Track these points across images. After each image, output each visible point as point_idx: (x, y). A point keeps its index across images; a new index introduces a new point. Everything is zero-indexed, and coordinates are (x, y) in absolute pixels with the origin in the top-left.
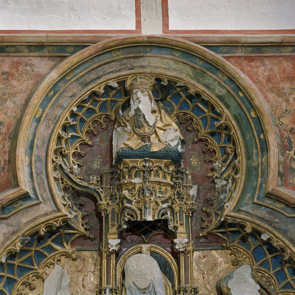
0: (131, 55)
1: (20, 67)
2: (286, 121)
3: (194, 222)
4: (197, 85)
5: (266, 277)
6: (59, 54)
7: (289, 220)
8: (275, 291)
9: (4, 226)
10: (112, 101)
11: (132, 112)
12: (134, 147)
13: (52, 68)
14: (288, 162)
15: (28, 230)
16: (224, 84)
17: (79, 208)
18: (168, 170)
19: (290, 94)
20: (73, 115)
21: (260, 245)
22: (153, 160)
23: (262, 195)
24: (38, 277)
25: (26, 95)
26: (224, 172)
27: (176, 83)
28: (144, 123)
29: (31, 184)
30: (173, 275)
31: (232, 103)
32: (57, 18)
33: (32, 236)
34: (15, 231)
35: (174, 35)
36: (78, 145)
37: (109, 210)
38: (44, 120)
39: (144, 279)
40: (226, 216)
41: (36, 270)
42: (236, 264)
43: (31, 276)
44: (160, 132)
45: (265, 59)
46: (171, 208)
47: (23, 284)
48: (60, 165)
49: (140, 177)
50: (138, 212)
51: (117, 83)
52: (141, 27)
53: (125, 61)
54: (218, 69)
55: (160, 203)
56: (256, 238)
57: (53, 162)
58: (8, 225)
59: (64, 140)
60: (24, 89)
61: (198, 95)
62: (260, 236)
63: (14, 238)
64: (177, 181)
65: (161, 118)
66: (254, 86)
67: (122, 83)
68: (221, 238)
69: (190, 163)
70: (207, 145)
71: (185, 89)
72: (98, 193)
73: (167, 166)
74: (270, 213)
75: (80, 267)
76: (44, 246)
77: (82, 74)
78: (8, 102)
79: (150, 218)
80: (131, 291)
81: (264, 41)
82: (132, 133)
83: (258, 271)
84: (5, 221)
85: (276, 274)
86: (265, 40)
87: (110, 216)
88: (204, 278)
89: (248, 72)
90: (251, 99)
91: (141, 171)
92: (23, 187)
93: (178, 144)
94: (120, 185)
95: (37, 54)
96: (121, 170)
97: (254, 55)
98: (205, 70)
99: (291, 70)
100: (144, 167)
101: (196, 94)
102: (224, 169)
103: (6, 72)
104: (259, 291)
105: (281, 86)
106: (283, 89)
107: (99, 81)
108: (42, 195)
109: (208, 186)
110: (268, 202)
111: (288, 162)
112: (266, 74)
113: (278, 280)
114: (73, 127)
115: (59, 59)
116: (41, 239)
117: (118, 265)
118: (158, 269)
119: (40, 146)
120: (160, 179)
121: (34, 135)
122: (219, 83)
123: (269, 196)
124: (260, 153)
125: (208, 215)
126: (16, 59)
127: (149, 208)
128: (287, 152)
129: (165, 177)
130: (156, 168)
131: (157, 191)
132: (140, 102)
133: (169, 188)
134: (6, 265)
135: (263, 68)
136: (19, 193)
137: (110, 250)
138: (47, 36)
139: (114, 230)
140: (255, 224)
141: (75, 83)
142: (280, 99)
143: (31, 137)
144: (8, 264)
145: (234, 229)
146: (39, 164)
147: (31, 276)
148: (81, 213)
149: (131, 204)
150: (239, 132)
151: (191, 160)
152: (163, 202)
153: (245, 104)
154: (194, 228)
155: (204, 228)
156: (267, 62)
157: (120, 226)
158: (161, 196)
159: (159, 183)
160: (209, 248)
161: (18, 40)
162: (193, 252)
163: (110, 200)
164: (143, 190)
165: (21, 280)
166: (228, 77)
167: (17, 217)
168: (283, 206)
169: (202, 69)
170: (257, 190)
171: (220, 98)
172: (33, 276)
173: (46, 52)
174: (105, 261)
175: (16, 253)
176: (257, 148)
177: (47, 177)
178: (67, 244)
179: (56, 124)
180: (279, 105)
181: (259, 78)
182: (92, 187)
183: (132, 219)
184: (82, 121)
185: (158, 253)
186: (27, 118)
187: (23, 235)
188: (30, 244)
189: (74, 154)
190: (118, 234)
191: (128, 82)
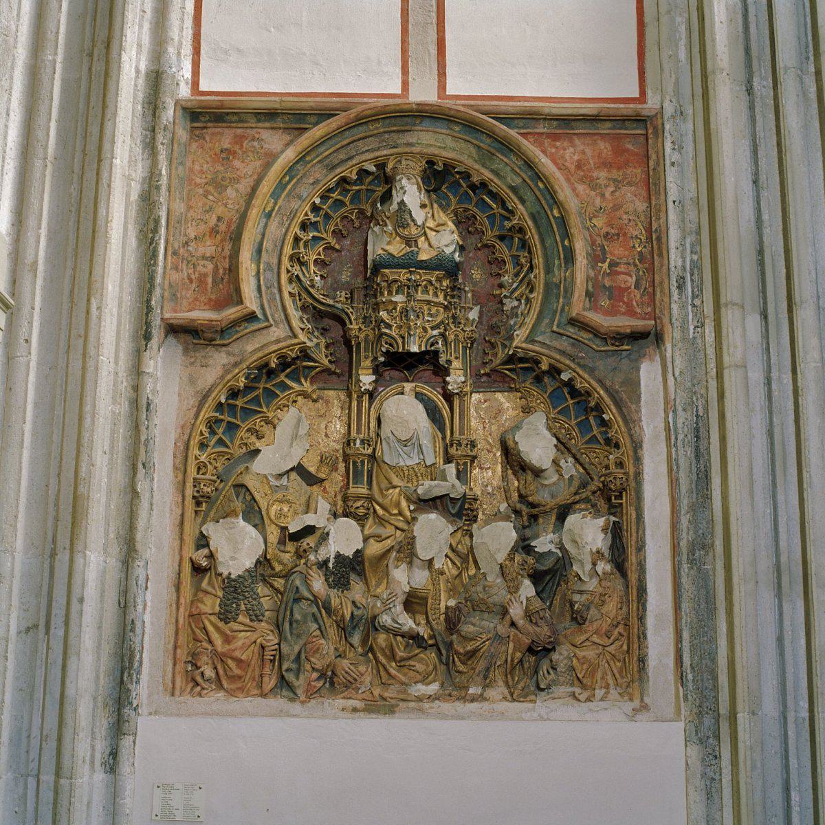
0: (395, 128)
1: (245, 142)
2: (599, 222)
3: (473, 355)
4: (483, 170)
5: (565, 429)
6: (297, 126)
7: (597, 354)
8: (577, 446)
9: (223, 355)
10: (367, 190)
11: (394, 206)
12: (395, 253)
13: (287, 145)
14: (600, 278)
15: (255, 361)
16: (518, 171)
17: (322, 334)
18: (441, 285)
19: (606, 186)
20: (315, 209)
21: (559, 387)
22: (421, 271)
23: (564, 320)
24: (268, 422)
25: (252, 180)
26: (515, 289)
27: (454, 168)
28: (410, 222)
29: (258, 301)
30: (445, 424)
31: (528, 196)
32: (295, 76)
33: (260, 368)
35: (453, 102)
36: (321, 249)
37: (362, 336)
38: (276, 215)
39: (405, 427)
40: (516, 348)
42: (527, 410)
43: (258, 420)
44: (431, 234)
45: (575, 138)
46: (443, 335)
47: (248, 430)
48: (297, 276)
49: (403, 294)
50: (400, 341)
51: (375, 166)
52: (408, 89)
53: (386, 136)
54: (511, 150)
55: (429, 329)
56: (554, 378)
57: (288, 271)
58: (228, 354)
59: (302, 242)
60: (250, 173)
61: (484, 185)
62: (559, 375)
63: (237, 371)
64: (452, 300)
65: (433, 215)
66: (558, 174)
67: (381, 166)
68: (509, 376)
69: (471, 277)
70: (494, 253)
71: (466, 175)
72: (347, 314)
73: (439, 280)
74: (573, 345)
75: (322, 412)
77: (327, 153)
78: (229, 190)
79: (414, 349)
80: (388, 443)
81: (574, 113)
82: (394, 235)
83: (555, 420)
84: (224, 349)
85: (578, 424)
86: (575, 112)
87: (362, 345)
88: (484, 427)
89: (552, 154)
90: (554, 192)
91: (405, 285)
92: (248, 305)
93: (455, 251)
94: (377, 304)
95: (267, 125)
96: (378, 285)
97: (561, 131)
98: (493, 151)
99: (609, 153)
100: (409, 280)
101: (481, 184)
102: (515, 285)
103: (226, 150)
104: (556, 446)
105: (595, 174)
106: (598, 179)
107: (350, 163)
108: (272, 316)
109: (494, 308)
110: (571, 331)
111: (600, 278)
112: (576, 158)
113: (581, 432)
114: (315, 225)
115: (296, 133)
116: (271, 373)
117: (372, 409)
118: (425, 415)
119: (270, 249)
120: (430, 297)
121: (263, 235)
122: (513, 169)
123: (573, 322)
124: (563, 265)
125: (493, 346)
126: (239, 131)
127: (414, 334)
128: (600, 264)
129: (436, 295)
130: (424, 283)
131: (426, 313)
132: (404, 193)
133: (442, 309)
134: (225, 406)
135: (572, 150)
137: (362, 390)
138: (282, 101)
139: (368, 363)
140: (554, 359)
141: (319, 165)
142: (593, 193)
143: (259, 237)
144: (228, 405)
145: (526, 365)
146: (269, 274)
147: (258, 420)
148: (324, 341)
149: (391, 330)
150: (536, 237)
151: (473, 272)
152: (433, 328)
153: (545, 199)
154: (474, 363)
155: (487, 363)
156: (577, 141)
157: (376, 359)
158: (430, 319)
159: (429, 302)
160: (493, 390)
161: (242, 105)
162: (471, 394)
163: (363, 323)
164: (407, 311)
165: (245, 426)
166: (525, 161)
168: (591, 336)
169: (490, 149)
170: (558, 315)
171: (514, 189)
172: (261, 421)
173: (279, 122)
174: (354, 404)
175: (239, 390)
176: (560, 258)
177: (280, 291)
178: (306, 380)
179: (292, 220)
180: (591, 201)
181: (566, 164)
182: (339, 306)
183: (392, 350)
184: (327, 217)
185: (425, 395)
186: (254, 213)
187: (248, 368)
188: (257, 379)
189: (315, 261)
190: (373, 369)
191: (390, 165)
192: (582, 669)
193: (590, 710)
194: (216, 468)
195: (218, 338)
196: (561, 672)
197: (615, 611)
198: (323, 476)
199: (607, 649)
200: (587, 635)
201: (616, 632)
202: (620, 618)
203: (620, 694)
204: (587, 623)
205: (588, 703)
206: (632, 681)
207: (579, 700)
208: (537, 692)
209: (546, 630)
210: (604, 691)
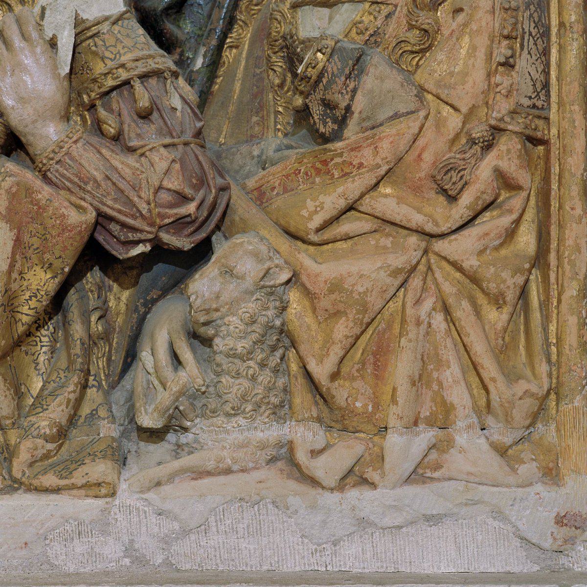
192: (328, 341)
193: (363, 523)
196: (232, 354)
197: (478, 76)
199: (439, 246)
200: (353, 187)
201: (484, 171)
202: (503, 107)
203: (502, 451)
204: (351, 131)
205: (353, 494)
206: (556, 391)
207: (314, 482)
208: (131, 445)
209: (162, 166)
210: (426, 436)
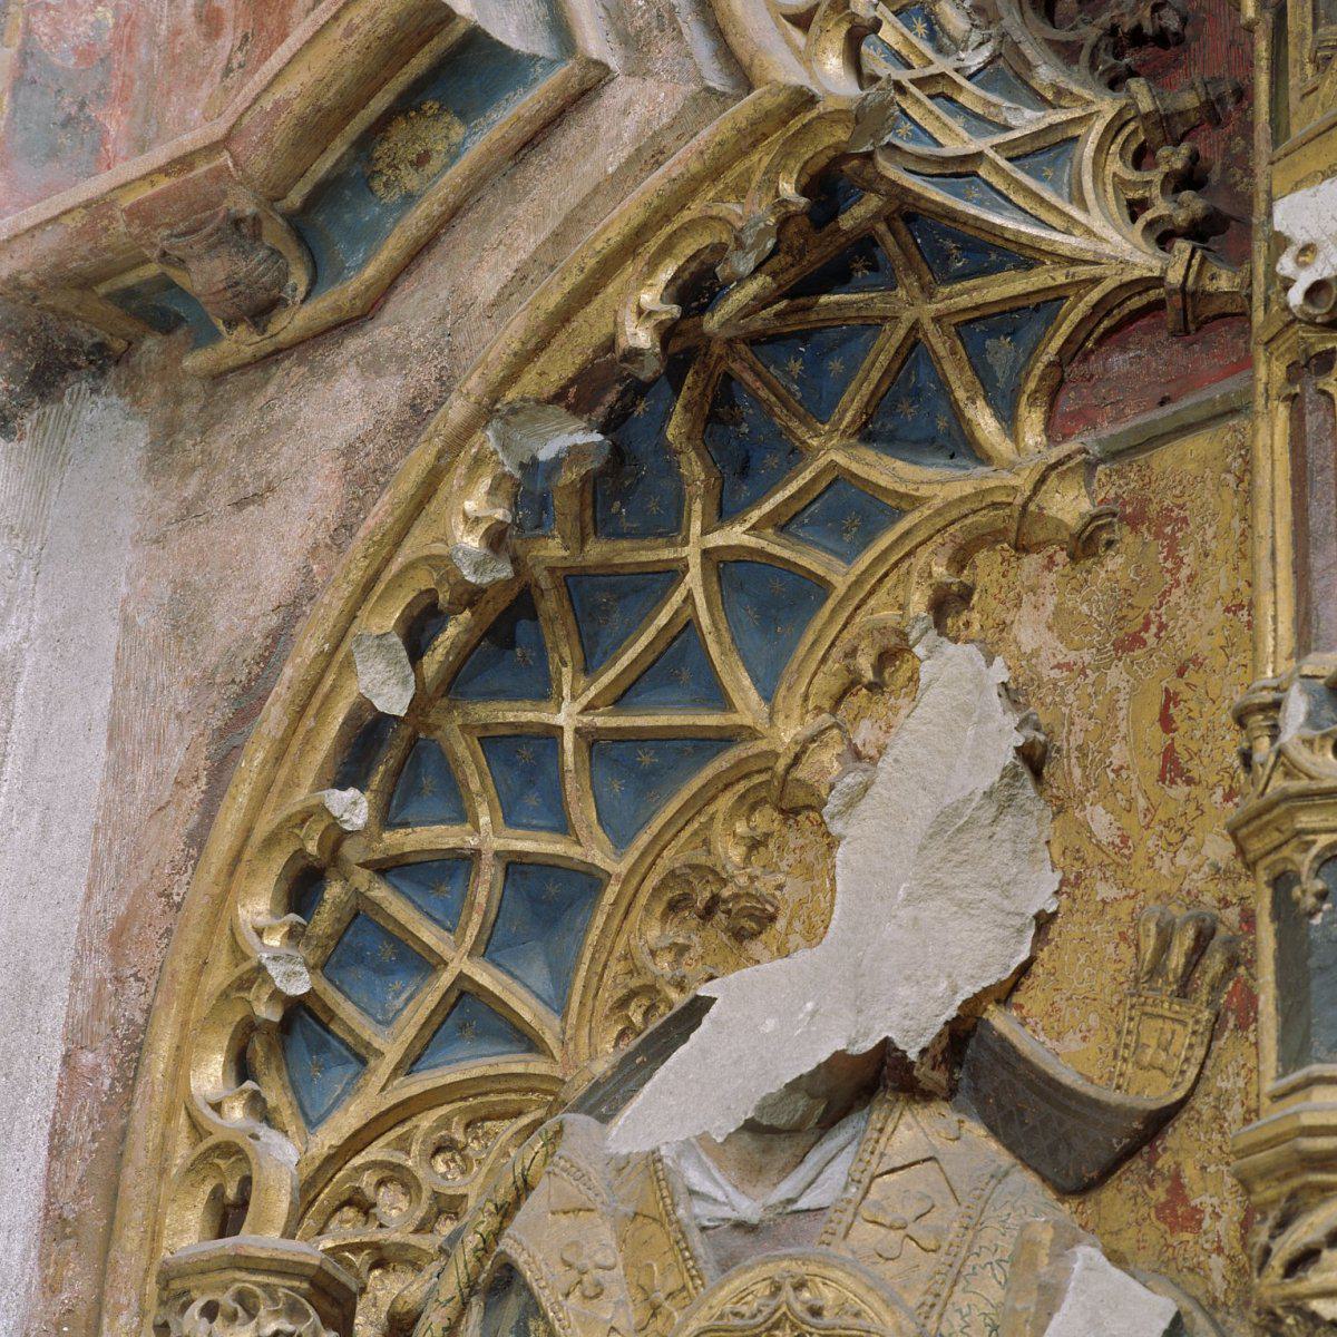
34: (422, 394)
41: (751, 734)
43: (725, 802)
76: (780, 497)
84: (355, 344)
136: (349, 33)
148: (1107, 107)
167: (442, 271)
178: (1009, 420)
194: (449, 1206)
195: (299, 278)
198: (1156, 1093)
